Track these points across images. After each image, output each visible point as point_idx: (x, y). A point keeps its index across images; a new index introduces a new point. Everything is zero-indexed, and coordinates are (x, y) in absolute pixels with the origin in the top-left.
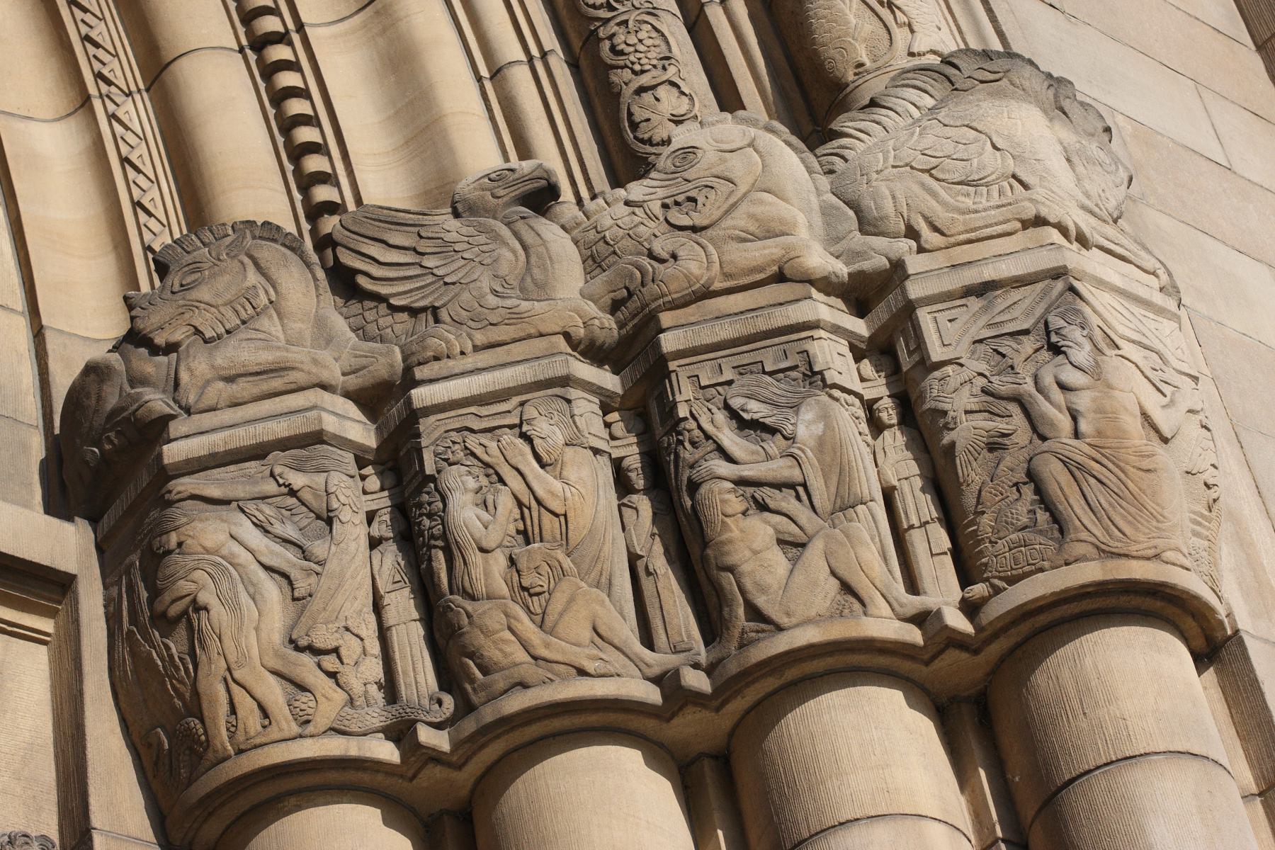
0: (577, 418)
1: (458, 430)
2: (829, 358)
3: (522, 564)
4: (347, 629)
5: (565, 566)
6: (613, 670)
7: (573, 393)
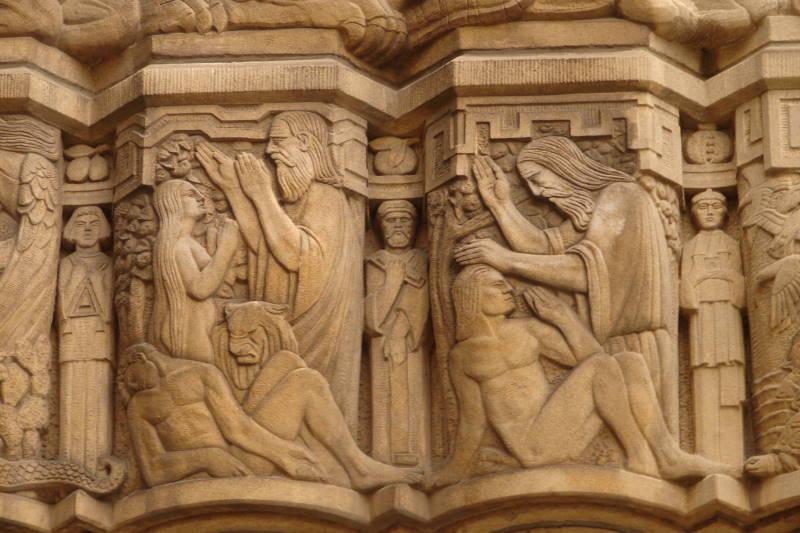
0: (334, 148)
1: (191, 133)
2: (649, 136)
3: (236, 323)
4: (15, 360)
5: (285, 337)
6: (318, 474)
7: (336, 113)
